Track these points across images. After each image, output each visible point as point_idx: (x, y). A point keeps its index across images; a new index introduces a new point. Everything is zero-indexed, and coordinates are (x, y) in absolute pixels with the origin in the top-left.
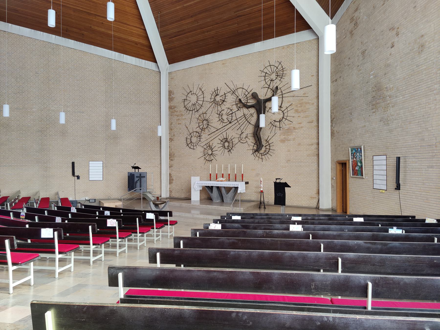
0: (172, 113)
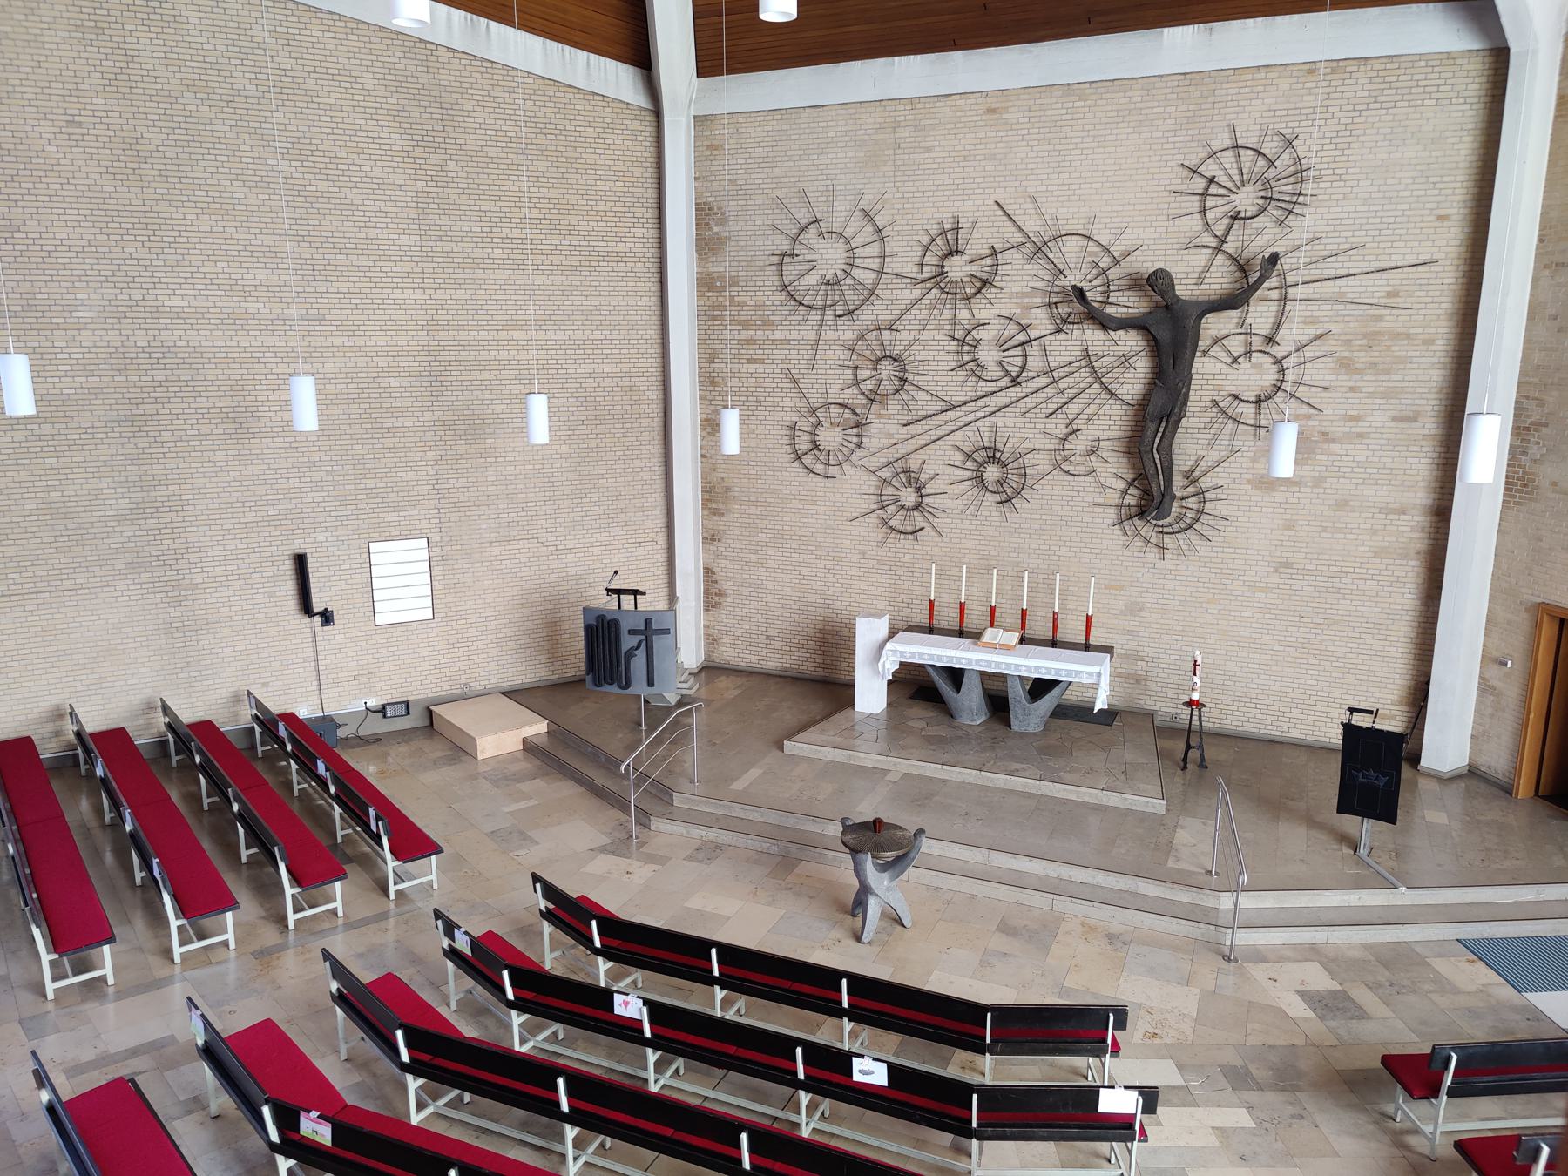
0: (713, 307)
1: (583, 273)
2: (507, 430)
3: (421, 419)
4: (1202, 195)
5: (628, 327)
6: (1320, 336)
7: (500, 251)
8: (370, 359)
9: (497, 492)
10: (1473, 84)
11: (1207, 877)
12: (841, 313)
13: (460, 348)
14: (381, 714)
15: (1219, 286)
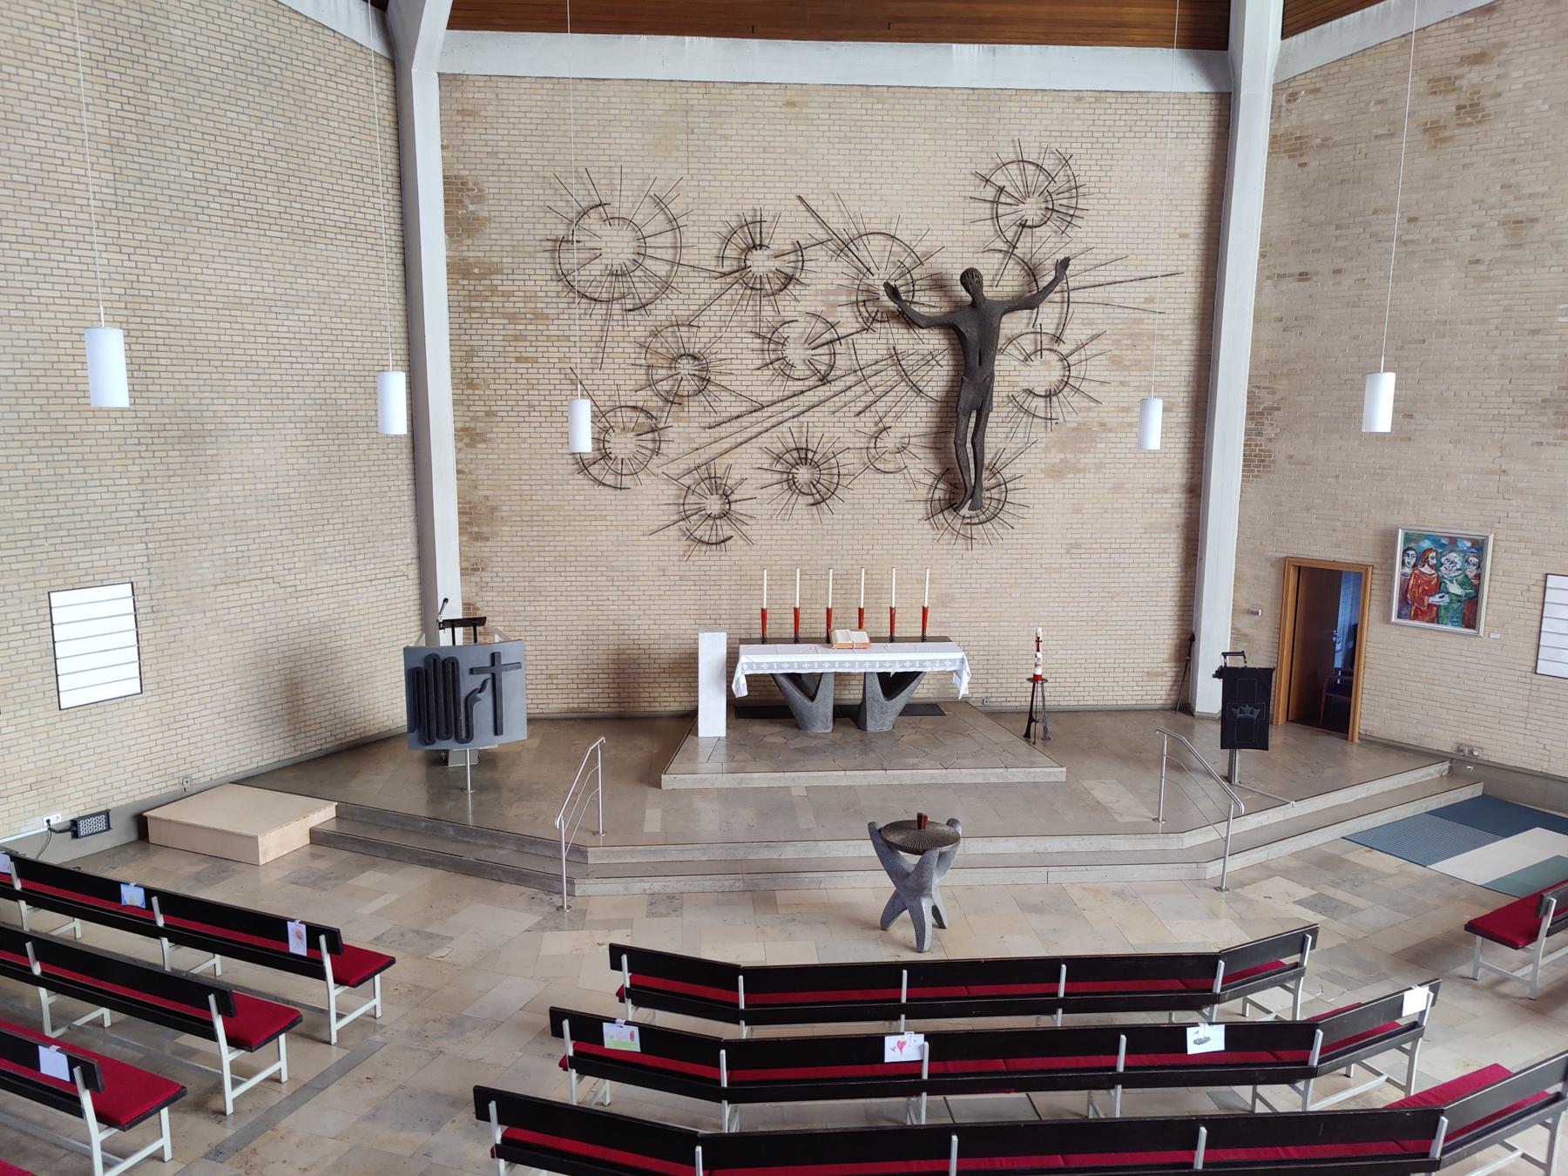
0: (470, 297)
1: (318, 246)
2: (232, 439)
3: (120, 421)
4: (992, 202)
5: (369, 316)
6: (1097, 336)
7: (218, 206)
8: (47, 336)
9: (223, 520)
10: (1202, 120)
11: (1155, 824)
12: (631, 307)
13: (169, 328)
14: (69, 834)
15: (1010, 289)
